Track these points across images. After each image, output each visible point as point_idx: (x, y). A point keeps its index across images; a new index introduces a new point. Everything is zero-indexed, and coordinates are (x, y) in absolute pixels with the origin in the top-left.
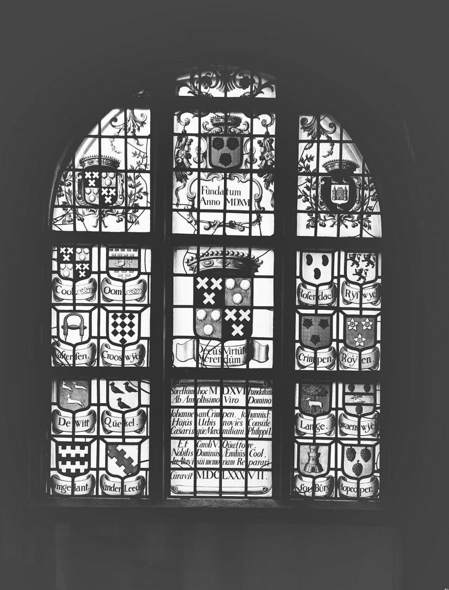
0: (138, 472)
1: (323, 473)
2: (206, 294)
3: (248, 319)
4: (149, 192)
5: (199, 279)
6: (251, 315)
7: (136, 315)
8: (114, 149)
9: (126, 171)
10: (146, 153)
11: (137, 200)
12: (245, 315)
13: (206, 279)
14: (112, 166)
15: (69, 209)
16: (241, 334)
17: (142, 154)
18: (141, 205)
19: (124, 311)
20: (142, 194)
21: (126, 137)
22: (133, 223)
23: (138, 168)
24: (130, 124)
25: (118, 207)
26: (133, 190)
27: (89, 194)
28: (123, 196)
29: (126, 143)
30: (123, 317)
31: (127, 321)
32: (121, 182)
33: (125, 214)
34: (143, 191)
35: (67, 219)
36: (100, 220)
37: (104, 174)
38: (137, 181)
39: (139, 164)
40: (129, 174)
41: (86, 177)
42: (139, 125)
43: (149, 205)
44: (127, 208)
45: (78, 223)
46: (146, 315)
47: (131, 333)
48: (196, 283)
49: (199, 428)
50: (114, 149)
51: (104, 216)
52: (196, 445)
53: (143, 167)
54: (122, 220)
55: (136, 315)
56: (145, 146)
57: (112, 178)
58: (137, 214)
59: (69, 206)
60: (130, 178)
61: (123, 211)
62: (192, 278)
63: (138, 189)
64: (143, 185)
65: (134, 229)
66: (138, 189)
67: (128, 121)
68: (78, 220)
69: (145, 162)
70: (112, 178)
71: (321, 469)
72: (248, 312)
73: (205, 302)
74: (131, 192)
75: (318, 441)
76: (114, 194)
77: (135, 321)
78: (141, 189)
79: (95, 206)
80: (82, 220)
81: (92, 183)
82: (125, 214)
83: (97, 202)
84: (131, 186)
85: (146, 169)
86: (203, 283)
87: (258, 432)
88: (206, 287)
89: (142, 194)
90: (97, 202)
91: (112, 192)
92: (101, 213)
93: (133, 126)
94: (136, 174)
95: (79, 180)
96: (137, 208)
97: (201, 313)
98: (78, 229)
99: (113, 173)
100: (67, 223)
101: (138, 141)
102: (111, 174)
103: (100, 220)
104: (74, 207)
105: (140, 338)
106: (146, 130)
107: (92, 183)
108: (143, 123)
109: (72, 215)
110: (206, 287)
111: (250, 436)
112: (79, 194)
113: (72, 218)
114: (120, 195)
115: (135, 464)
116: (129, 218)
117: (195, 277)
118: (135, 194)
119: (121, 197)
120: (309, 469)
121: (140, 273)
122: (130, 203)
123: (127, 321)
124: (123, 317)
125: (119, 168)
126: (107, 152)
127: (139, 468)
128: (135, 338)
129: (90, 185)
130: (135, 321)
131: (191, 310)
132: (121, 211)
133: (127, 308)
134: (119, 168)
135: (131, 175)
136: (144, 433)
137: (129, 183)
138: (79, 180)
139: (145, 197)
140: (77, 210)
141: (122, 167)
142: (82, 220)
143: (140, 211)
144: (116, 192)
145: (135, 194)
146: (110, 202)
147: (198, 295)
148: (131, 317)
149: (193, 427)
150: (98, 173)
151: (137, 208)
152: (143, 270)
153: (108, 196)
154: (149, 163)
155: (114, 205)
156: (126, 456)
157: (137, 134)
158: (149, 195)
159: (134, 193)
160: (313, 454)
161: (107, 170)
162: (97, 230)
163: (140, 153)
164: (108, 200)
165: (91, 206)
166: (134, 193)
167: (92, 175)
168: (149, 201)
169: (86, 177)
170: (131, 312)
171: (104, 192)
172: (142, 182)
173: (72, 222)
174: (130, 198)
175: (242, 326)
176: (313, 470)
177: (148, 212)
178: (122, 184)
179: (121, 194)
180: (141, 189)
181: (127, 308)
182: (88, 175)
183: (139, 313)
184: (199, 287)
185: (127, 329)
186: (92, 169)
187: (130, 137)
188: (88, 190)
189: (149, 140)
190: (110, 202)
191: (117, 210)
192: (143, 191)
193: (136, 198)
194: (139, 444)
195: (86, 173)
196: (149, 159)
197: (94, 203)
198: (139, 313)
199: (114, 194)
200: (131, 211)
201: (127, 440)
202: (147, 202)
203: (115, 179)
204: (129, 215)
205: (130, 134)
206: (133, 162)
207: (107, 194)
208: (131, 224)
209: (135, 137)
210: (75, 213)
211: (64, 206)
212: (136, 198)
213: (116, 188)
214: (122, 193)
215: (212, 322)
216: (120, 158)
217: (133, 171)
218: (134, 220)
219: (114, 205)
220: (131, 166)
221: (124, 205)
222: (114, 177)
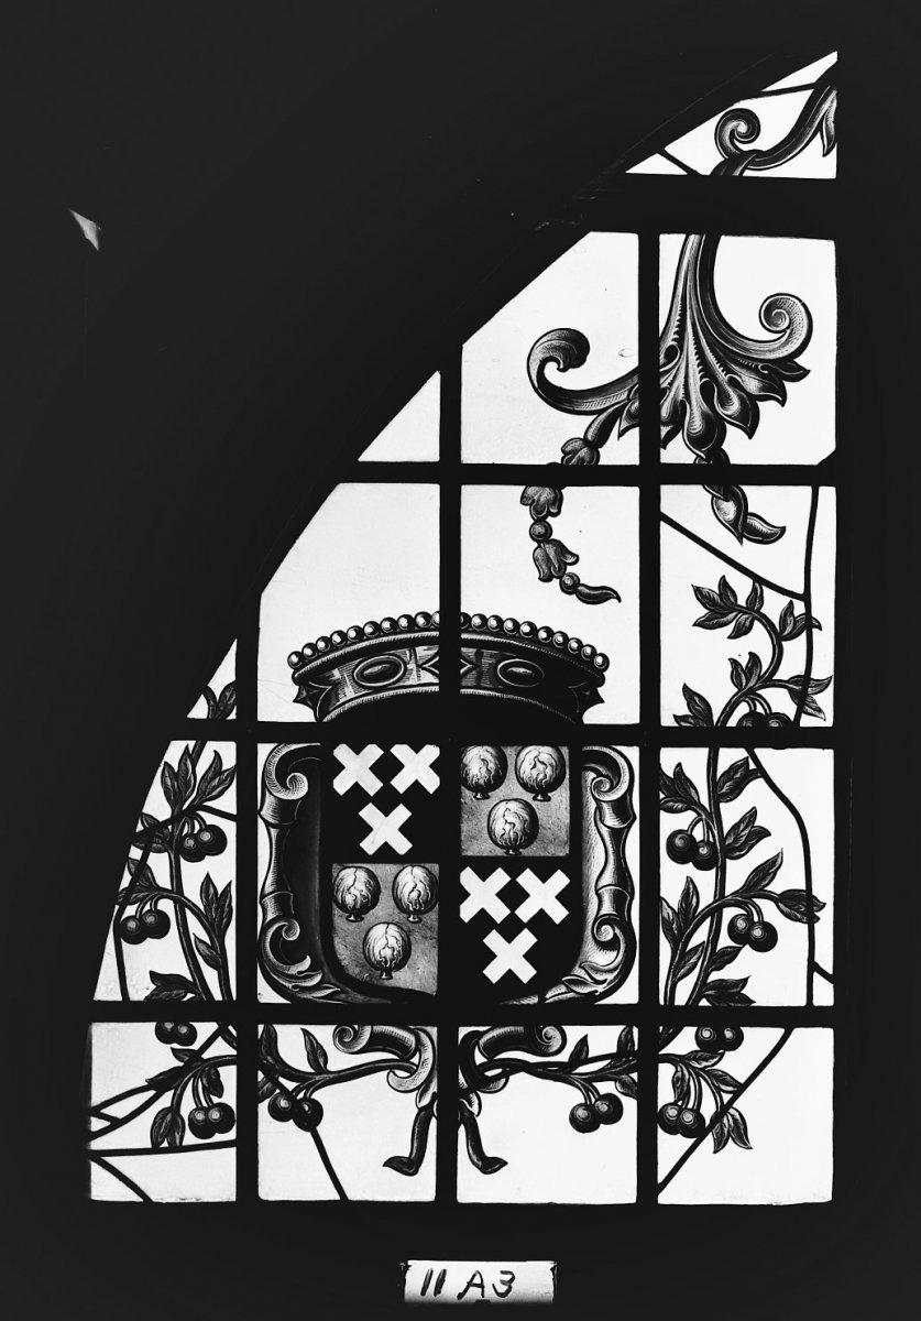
4: (824, 889)
8: (555, 562)
9: (649, 733)
10: (806, 597)
11: (729, 956)
14: (542, 688)
15: (205, 1029)
17: (773, 606)
18: (762, 994)
20: (770, 912)
21: (649, 477)
22: (697, 1131)
23: (743, 709)
24: (684, 378)
25: (590, 1011)
26: (706, 881)
27: (359, 912)
28: (626, 927)
29: (651, 519)
32: (611, 820)
33: (636, 1064)
34: (778, 886)
35: (187, 1106)
36: (449, 1116)
37: (477, 761)
38: (731, 813)
39: (749, 677)
40: (669, 758)
41: (341, 785)
42: (752, 384)
43: (825, 995)
44: (652, 1021)
45: (278, 1140)
50: (555, 562)
51: (481, 1083)
53: (780, 701)
54: (615, 1114)
56: (801, 544)
57: (543, 790)
58: (735, 1064)
59: (206, 1008)
60: (679, 788)
61: (624, 1042)
63: (738, 872)
64: (782, 838)
65: (704, 1179)
66: (738, 872)
67: (672, 353)
68: (278, 1114)
69: (792, 666)
70: (543, 790)
74: (690, 891)
76: (558, 913)
78: (768, 869)
79: (409, 1007)
80: (309, 1117)
81: (386, 829)
82: (636, 1064)
83: (420, 974)
84: (685, 851)
85: (807, 721)
89: (770, 912)
90: (420, 974)
91: (544, 896)
92: (451, 1057)
93: (706, 391)
94: (729, 757)
95: (283, 807)
96: (729, 1013)
98: (275, 1185)
99: (546, 753)
100: (190, 1139)
101: (742, 503)
102: (535, 760)
103: (449, 1116)
104: (241, 1016)
106: (802, 425)
107: (386, 829)
108: (781, 374)
109: (228, 1075)
112: (284, 912)
113: (230, 1097)
114: (602, 920)
116: (666, 1094)
118: (715, 912)
119: (608, 933)
122: (676, 974)
125: (593, 716)
126: (505, 587)
129: (370, 845)
132: (604, 1039)
134: (593, 716)
135: (691, 761)
137: (670, 823)
138: (283, 807)
139: (791, 934)
140: (272, 1038)
141: (617, 704)
142: (309, 1117)
143: (758, 1040)
144: (572, 897)
145: (715, 912)
146: (526, 973)
150: (431, 752)
151: (729, 1013)
153: (510, 929)
154: (824, 667)
155: (556, 993)
157: (739, 448)
158: (826, 918)
159: (706, 897)
161: (507, 730)
162: (421, 1187)
163: (756, 598)
164: (510, 958)
165: (366, 1005)
166: (706, 897)
167: (387, 768)
168: (826, 959)
169: (341, 785)
171: (481, 895)
172: (772, 815)
173: (232, 1135)
174: (679, 941)
177: (815, 1048)
178: (618, 837)
179: (607, 909)
180: (768, 869)
182: (355, 768)
186: (387, 723)
187: (681, 475)
188: (353, 883)
189: (828, 495)
190: (526, 973)
191: (574, 1033)
192: (778, 886)
193: (725, 941)
195: (342, 753)
196: (825, 641)
197: (403, 979)
199: (558, 913)
200: (685, 1042)
202: (813, 967)
203: (561, 797)
204: (666, 1072)
205: (677, 452)
206: (701, 664)
207: (499, 912)
208: (681, 1143)
209: (724, 479)
210: (257, 1057)
211: (169, 1007)
212: (725, 941)
213: (574, 863)
214: (621, 900)
216: (610, 633)
217: (701, 729)
218: (708, 1109)
219: (556, 993)
220: (688, 692)
221: (629, 994)
222: (555, 784)
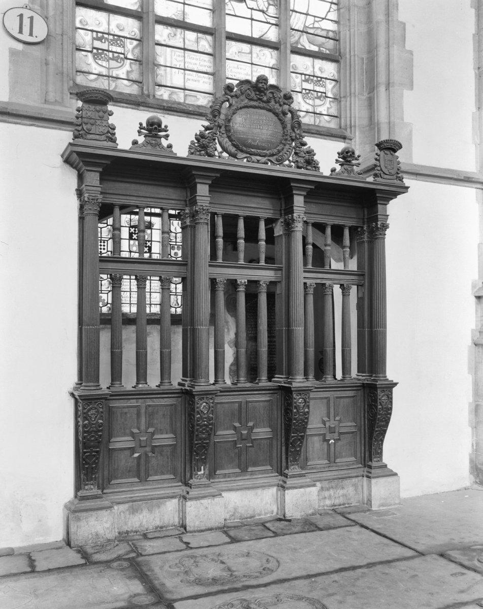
0: (107, 305)
1: (179, 306)
2: (133, 235)
3: (150, 245)
5: (131, 229)
6: (151, 244)
7: (106, 242)
12: (149, 244)
13: (134, 229)
16: (147, 251)
19: (101, 240)
30: (101, 242)
31: (102, 244)
46: (110, 242)
47: (104, 249)
48: (130, 230)
49: (131, 287)
52: (130, 294)
55: (106, 242)
62: (128, 228)
71: (178, 305)
72: (150, 242)
73: (133, 238)
75: (177, 294)
77: (106, 244)
86: (132, 230)
87: (155, 289)
88: (134, 232)
97: (132, 242)
105: (108, 251)
110: (134, 232)
111: (152, 291)
115: (106, 301)
117: (129, 227)
120: (174, 304)
121: (108, 225)
123: (102, 244)
124: (101, 242)
127: (108, 303)
128: (105, 251)
130: (106, 244)
131: (128, 241)
133: (102, 239)
136: (109, 289)
147: (131, 235)
148: (104, 242)
149: (129, 287)
152: (109, 224)
156: (102, 298)
160: (176, 299)
170: (104, 240)
175: (147, 248)
176: (175, 305)
181: (102, 239)
183: (107, 241)
184: (131, 232)
185: (102, 247)
194: (107, 293)
198: (107, 241)
201: (103, 292)
215: (136, 246)
